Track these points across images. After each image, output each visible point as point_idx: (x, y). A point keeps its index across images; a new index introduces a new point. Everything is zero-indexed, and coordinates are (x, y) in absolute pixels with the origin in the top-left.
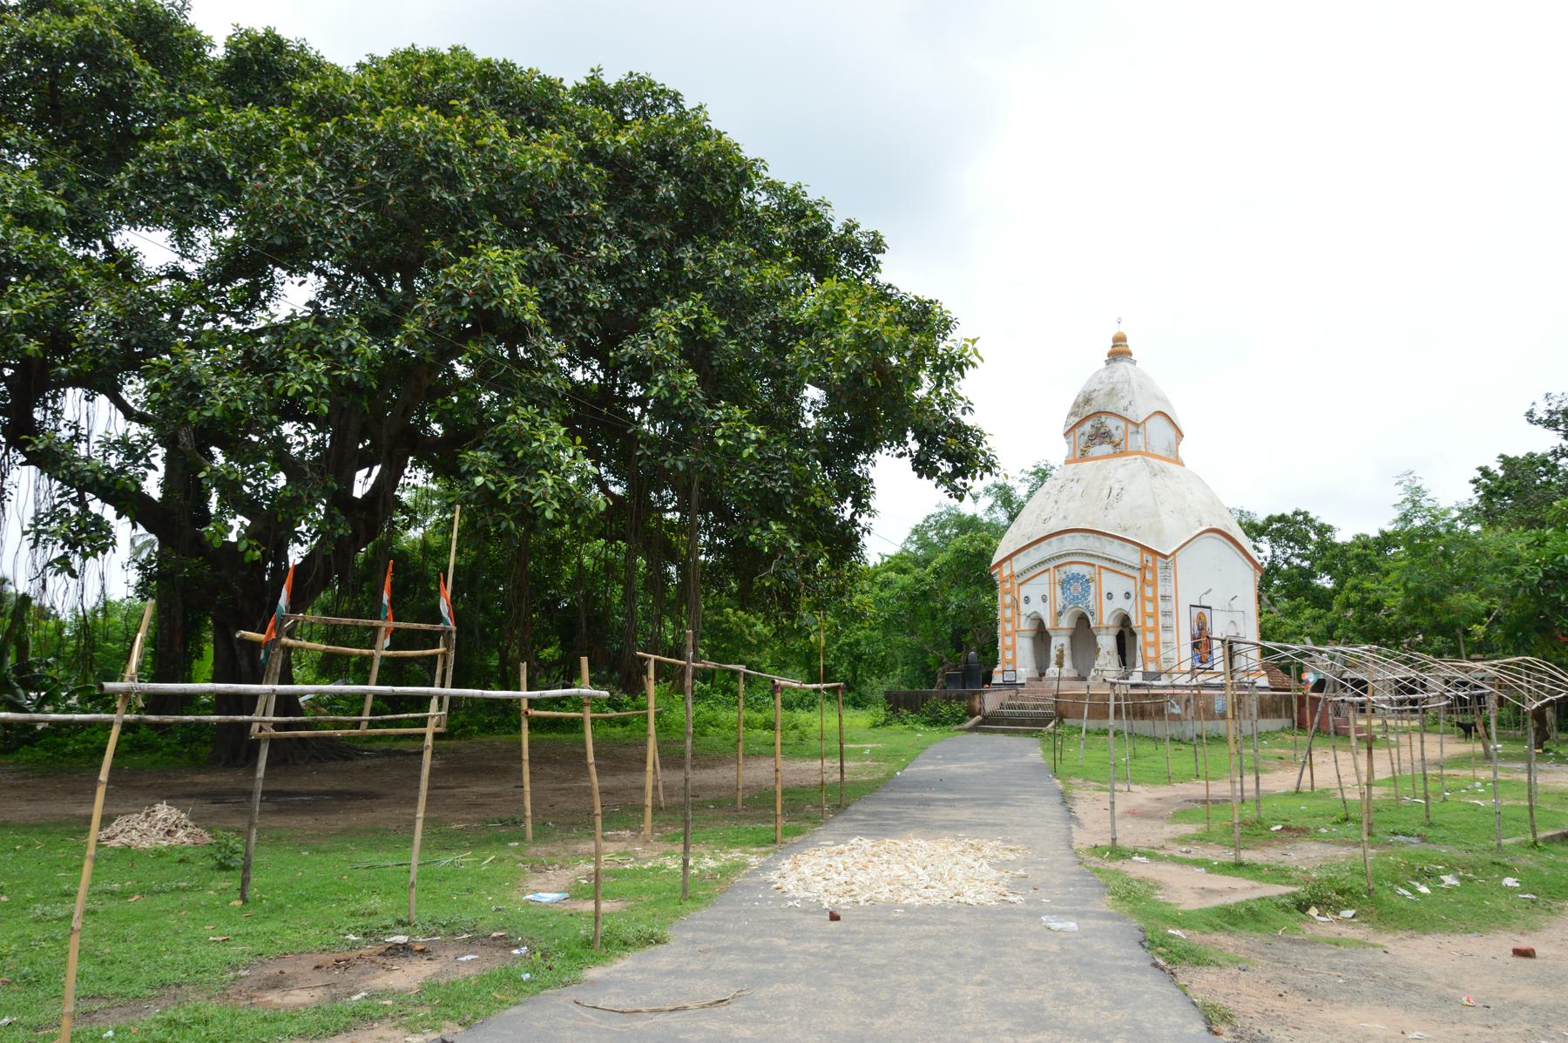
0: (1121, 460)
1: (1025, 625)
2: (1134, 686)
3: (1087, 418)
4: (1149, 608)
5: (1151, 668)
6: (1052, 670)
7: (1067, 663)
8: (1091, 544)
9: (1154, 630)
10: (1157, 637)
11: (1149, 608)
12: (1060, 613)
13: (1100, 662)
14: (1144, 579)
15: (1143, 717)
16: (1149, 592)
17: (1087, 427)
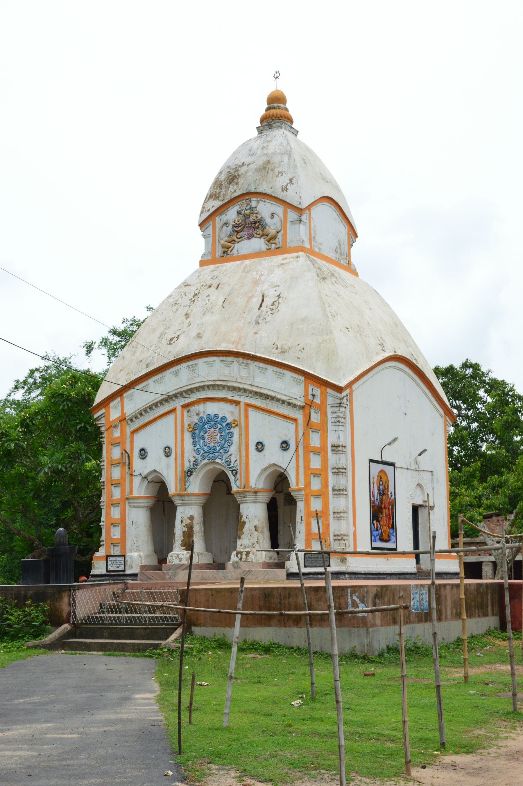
0: (278, 259)
1: (139, 489)
2: (291, 576)
3: (232, 201)
4: (316, 463)
6: (178, 554)
7: (199, 546)
9: (321, 495)
11: (316, 463)
12: (189, 473)
13: (244, 542)
14: (308, 422)
16: (315, 440)
17: (231, 215)
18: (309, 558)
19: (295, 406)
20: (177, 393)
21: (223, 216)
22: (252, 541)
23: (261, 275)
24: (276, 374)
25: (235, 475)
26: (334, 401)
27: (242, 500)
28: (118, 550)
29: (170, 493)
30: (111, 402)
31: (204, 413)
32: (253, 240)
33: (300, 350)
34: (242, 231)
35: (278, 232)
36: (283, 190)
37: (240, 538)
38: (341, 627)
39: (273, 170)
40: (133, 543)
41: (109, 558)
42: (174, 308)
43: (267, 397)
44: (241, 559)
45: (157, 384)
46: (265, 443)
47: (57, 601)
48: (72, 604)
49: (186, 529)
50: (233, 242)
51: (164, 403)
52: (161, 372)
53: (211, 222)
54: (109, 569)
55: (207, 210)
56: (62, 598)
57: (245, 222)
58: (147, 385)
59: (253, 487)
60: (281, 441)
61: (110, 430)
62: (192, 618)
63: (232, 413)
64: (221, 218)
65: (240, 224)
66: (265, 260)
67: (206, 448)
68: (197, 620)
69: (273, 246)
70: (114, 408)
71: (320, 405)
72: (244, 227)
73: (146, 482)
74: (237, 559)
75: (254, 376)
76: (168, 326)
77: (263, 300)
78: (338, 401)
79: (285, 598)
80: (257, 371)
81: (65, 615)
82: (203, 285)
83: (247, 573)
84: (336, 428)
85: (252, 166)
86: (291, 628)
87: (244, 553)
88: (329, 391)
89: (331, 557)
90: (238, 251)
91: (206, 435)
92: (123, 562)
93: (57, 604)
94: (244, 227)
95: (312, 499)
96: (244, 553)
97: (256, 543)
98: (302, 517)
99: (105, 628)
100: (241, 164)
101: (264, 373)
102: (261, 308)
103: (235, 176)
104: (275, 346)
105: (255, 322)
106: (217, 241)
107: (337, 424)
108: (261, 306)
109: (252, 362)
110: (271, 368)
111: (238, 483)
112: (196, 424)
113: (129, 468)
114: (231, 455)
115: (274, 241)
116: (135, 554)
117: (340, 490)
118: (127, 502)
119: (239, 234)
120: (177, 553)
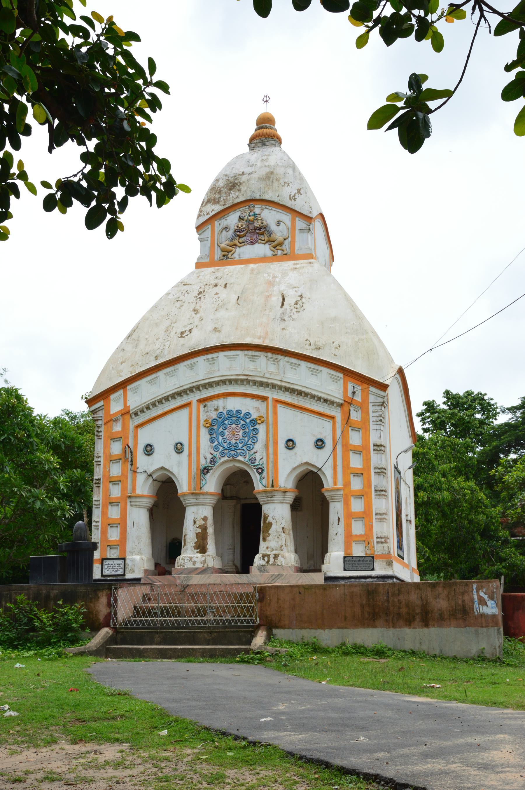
1: (144, 488)
4: (356, 462)
5: (358, 551)
6: (188, 557)
8: (263, 367)
10: (368, 506)
11: (356, 462)
12: (206, 470)
14: (347, 419)
15: (426, 623)
16: (355, 438)
17: (233, 220)
19: (332, 403)
20: (193, 387)
21: (222, 221)
22: (280, 543)
23: (274, 277)
24: (310, 371)
25: (260, 474)
26: (377, 399)
27: (268, 500)
28: (115, 553)
29: (179, 492)
30: (111, 394)
31: (224, 408)
32: (257, 245)
33: (336, 348)
34: (245, 235)
35: (285, 239)
36: (290, 199)
37: (264, 540)
38: (466, 627)
39: (278, 180)
40: (134, 546)
42: (178, 304)
43: (300, 393)
44: (268, 562)
45: (168, 377)
46: (296, 440)
47: (91, 602)
48: (112, 605)
49: (199, 530)
50: (234, 246)
51: (176, 396)
52: (174, 365)
53: (210, 226)
54: (104, 574)
55: (205, 213)
56: (99, 598)
57: (249, 228)
58: (156, 377)
59: (282, 485)
60: (315, 439)
61: (109, 424)
62: (274, 619)
63: (258, 409)
64: (220, 222)
65: (243, 229)
66: (272, 264)
67: (225, 445)
68: (280, 621)
69: (279, 252)
70: (115, 401)
71: (361, 404)
72: (247, 233)
73: (151, 480)
74: (262, 562)
75: (284, 371)
76: (174, 321)
77: (284, 299)
78: (381, 400)
79: (394, 595)
80: (288, 366)
81: (101, 617)
82: (206, 285)
83: (276, 577)
84: (378, 427)
85: (253, 175)
86: (402, 629)
87: (272, 557)
88: (372, 389)
89: (375, 560)
90: (239, 255)
91: (226, 431)
92: (122, 566)
93: (92, 605)
94: (247, 233)
95: (352, 498)
96: (272, 557)
97: (284, 545)
98: (339, 519)
99: (157, 633)
100: (241, 173)
101: (296, 369)
102: (284, 307)
103: (237, 184)
104: (308, 342)
105: (280, 319)
106: (216, 245)
107: (379, 423)
108: (283, 304)
109: (282, 357)
110: (304, 364)
111: (264, 482)
113: (132, 465)
114: (255, 453)
115: (280, 248)
116: (138, 557)
117: (382, 491)
118: (128, 501)
119: (241, 239)
120: (190, 555)
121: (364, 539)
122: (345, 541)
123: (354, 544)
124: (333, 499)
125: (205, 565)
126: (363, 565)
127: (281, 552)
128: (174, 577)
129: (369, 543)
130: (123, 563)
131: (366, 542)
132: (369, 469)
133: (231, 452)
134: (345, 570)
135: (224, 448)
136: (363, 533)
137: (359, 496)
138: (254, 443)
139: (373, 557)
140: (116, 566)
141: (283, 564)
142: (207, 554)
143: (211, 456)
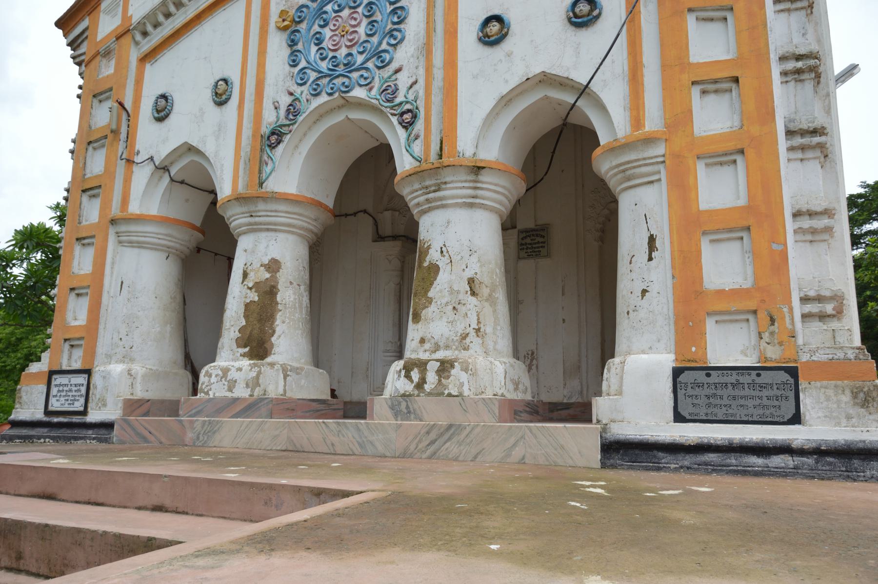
2: (619, 451)
5: (729, 346)
6: (229, 369)
7: (289, 341)
10: (766, 186)
12: (275, 137)
13: (432, 329)
18: (700, 385)
22: (460, 328)
25: (407, 126)
37: (417, 318)
40: (116, 339)
41: (54, 377)
44: (420, 386)
46: (511, 17)
49: (254, 297)
59: (469, 153)
73: (166, 180)
83: (442, 435)
87: (433, 367)
92: (83, 390)
95: (700, 167)
96: (433, 367)
97: (473, 334)
98: (652, 240)
111: (417, 148)
112: (303, 6)
116: (117, 368)
118: (112, 231)
121: (752, 305)
122: (676, 315)
123: (710, 325)
124: (629, 179)
125: (257, 392)
126: (750, 403)
127: (463, 355)
128: (181, 421)
129: (773, 321)
130: (85, 383)
131: (763, 315)
132: (762, 56)
133: (335, 81)
134: (679, 418)
135: (320, 72)
136: (748, 284)
137: (724, 154)
138: (395, 46)
139: (793, 372)
140: (74, 388)
141: (466, 393)
142: (269, 360)
143: (288, 100)
